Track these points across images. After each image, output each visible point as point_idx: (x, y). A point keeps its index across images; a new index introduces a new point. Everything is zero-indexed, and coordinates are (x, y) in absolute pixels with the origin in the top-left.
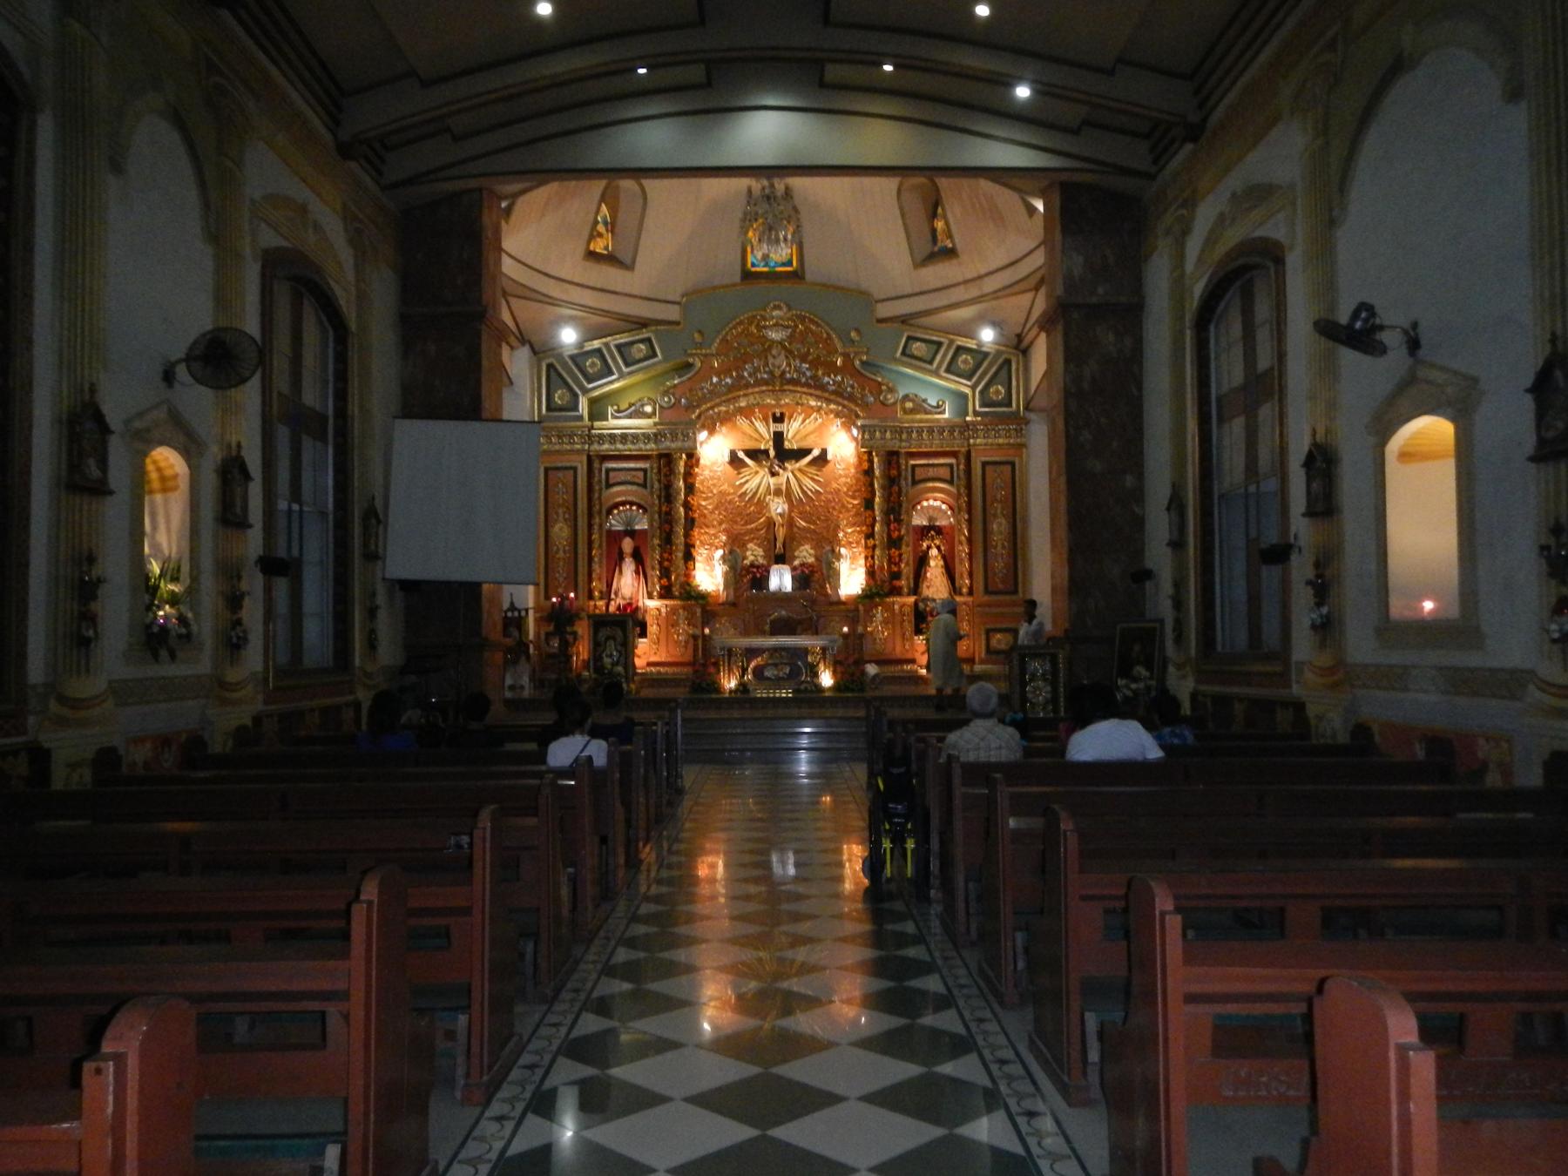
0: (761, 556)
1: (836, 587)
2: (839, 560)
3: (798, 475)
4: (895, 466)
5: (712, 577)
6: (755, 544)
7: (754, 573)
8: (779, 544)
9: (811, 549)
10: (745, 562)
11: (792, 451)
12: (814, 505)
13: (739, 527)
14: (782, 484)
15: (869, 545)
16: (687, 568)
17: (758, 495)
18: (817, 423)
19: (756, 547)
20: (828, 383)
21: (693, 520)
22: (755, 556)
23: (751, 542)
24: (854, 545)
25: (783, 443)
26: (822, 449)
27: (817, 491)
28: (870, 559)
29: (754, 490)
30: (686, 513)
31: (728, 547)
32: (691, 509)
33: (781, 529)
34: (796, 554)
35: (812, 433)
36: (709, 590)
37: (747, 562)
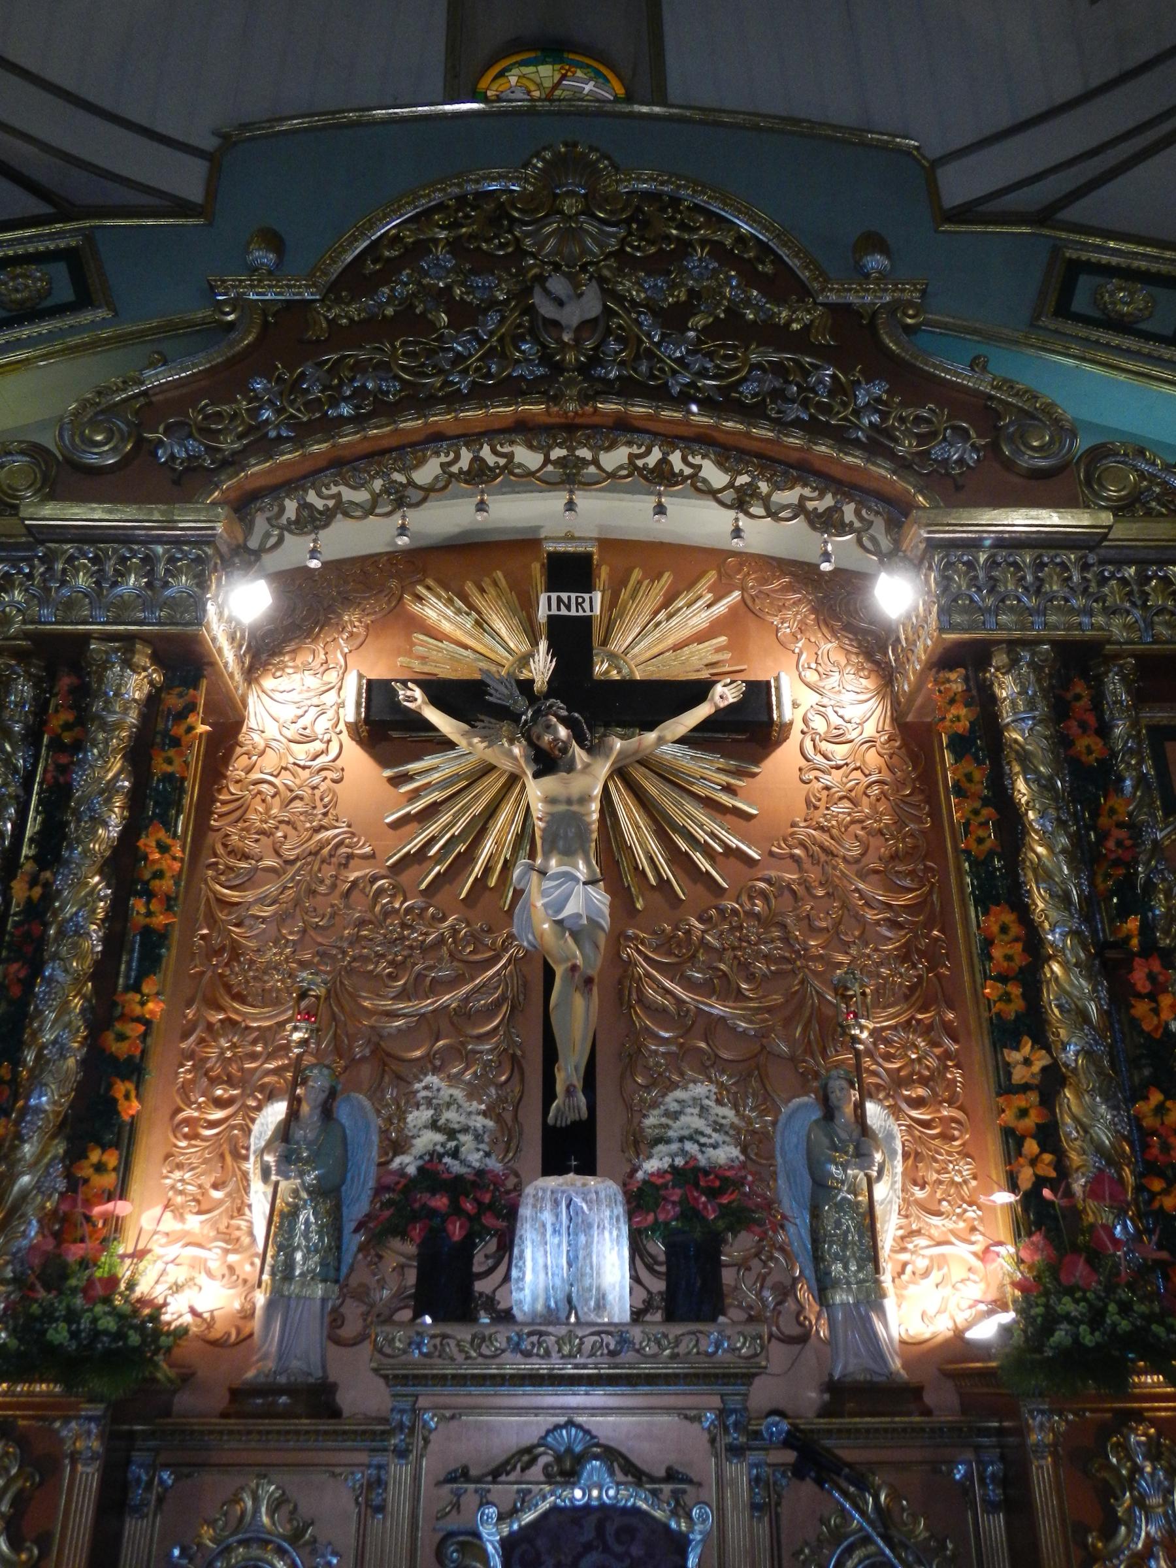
0: (478, 1138)
1: (873, 1298)
2: (862, 1156)
3: (652, 787)
4: (1092, 720)
5: (230, 1240)
6: (453, 1080)
7: (433, 1213)
8: (568, 1073)
9: (719, 1102)
10: (398, 1161)
11: (628, 686)
12: (721, 911)
13: (387, 1005)
14: (584, 799)
15: (1020, 1075)
16: (74, 1183)
17: (478, 869)
18: (721, 608)
19: (458, 1094)
20: (778, 394)
21: (153, 941)
22: (451, 1134)
23: (436, 1070)
24: (921, 1092)
25: (590, 665)
26: (750, 684)
27: (729, 851)
28: (1031, 1146)
29: (462, 848)
30: (118, 912)
31: (319, 1081)
32: (149, 895)
33: (579, 1001)
34: (652, 1119)
35: (701, 637)
36: (176, 1313)
37: (408, 1163)
